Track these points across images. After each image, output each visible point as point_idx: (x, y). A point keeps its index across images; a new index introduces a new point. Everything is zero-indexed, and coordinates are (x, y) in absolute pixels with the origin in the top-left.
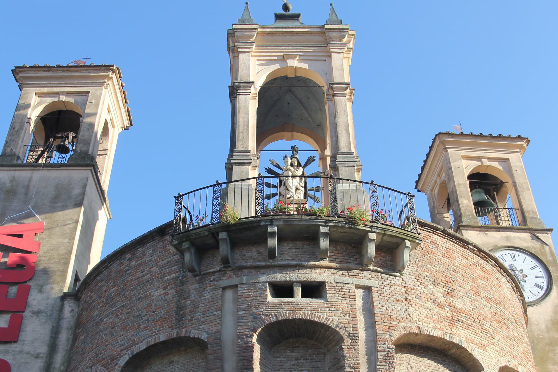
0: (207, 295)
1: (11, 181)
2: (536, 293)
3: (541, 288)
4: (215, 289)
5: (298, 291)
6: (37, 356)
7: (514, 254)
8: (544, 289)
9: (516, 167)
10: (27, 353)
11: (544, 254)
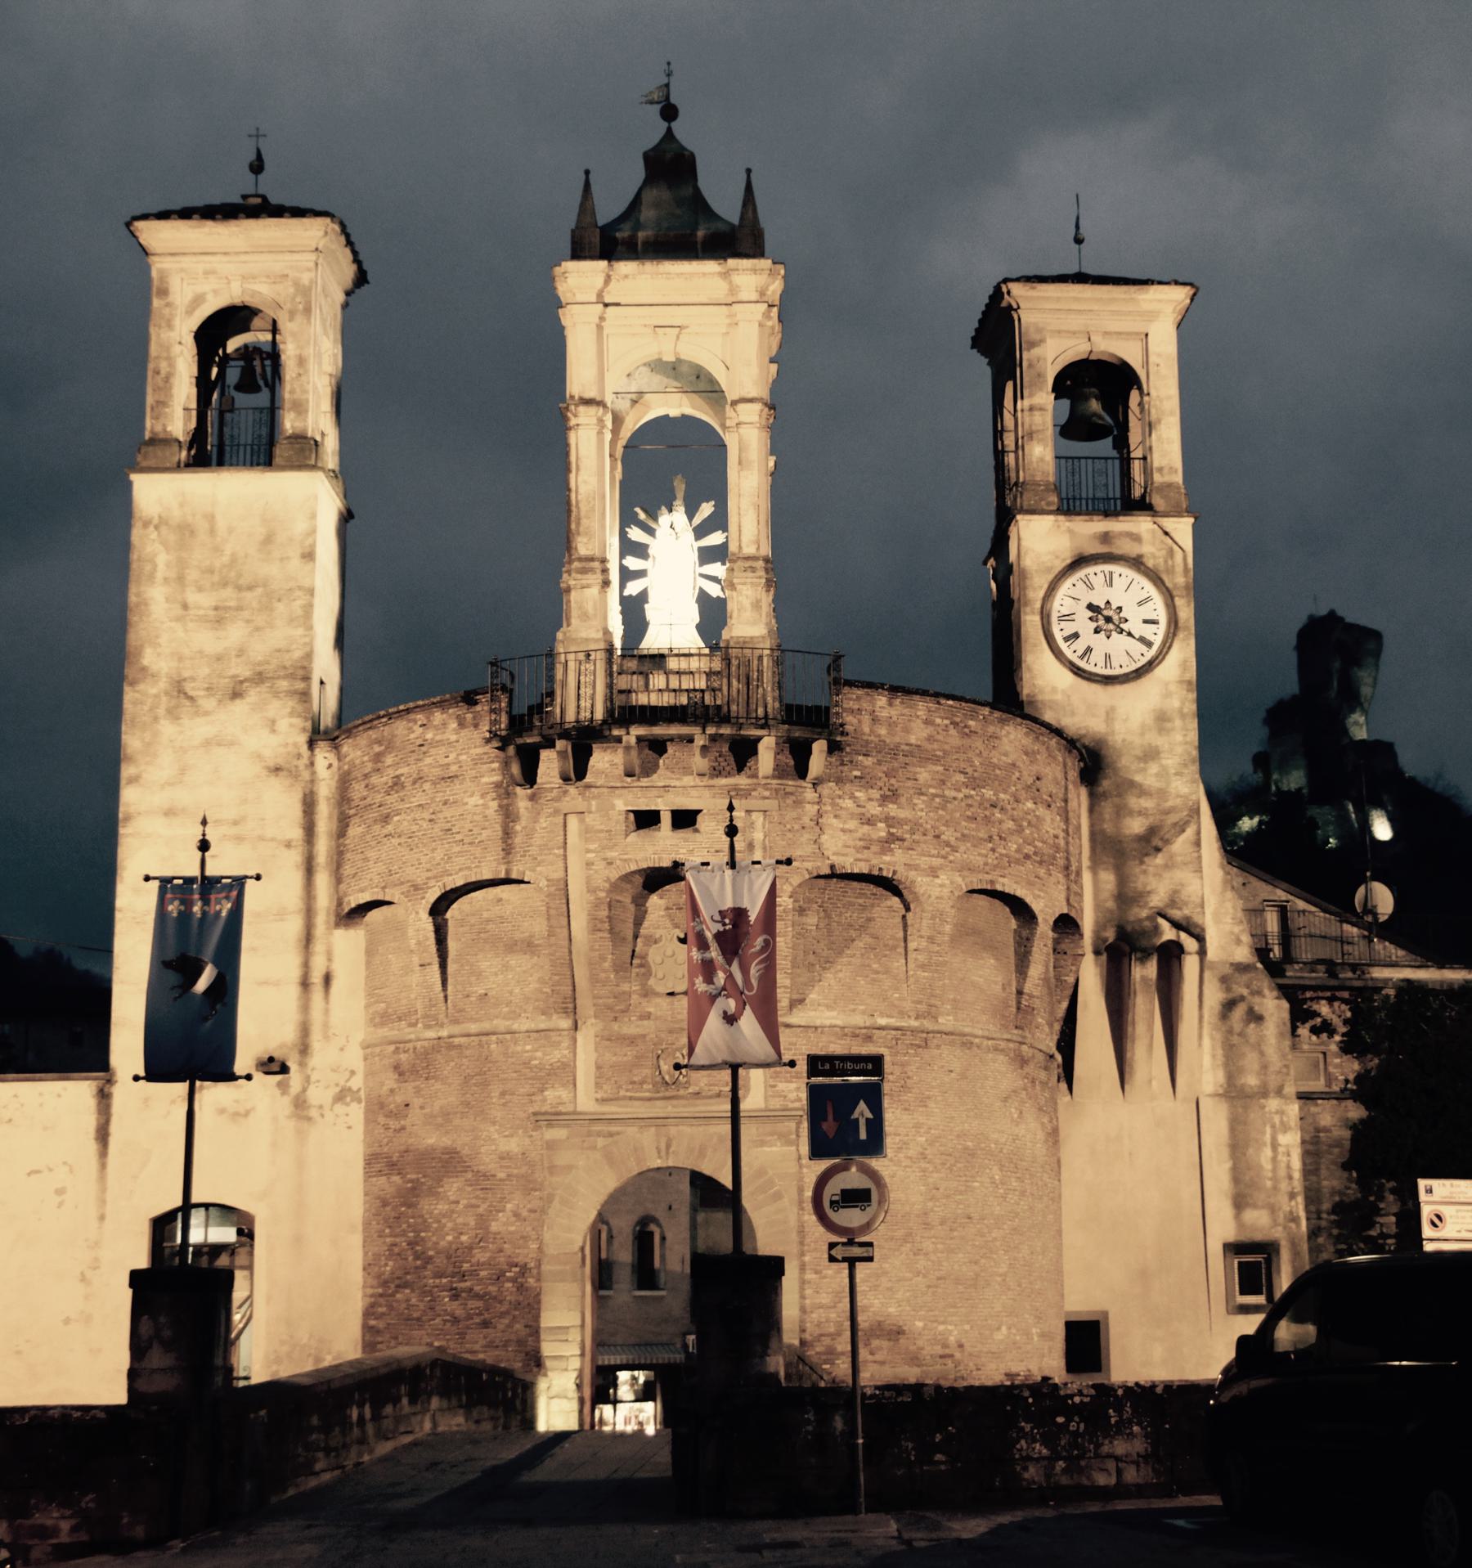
0: (543, 822)
1: (181, 505)
2: (1137, 656)
3: (1149, 644)
4: (556, 812)
5: (666, 819)
6: (288, 845)
7: (1111, 573)
8: (1155, 648)
9: (1159, 355)
10: (273, 839)
11: (1171, 571)
